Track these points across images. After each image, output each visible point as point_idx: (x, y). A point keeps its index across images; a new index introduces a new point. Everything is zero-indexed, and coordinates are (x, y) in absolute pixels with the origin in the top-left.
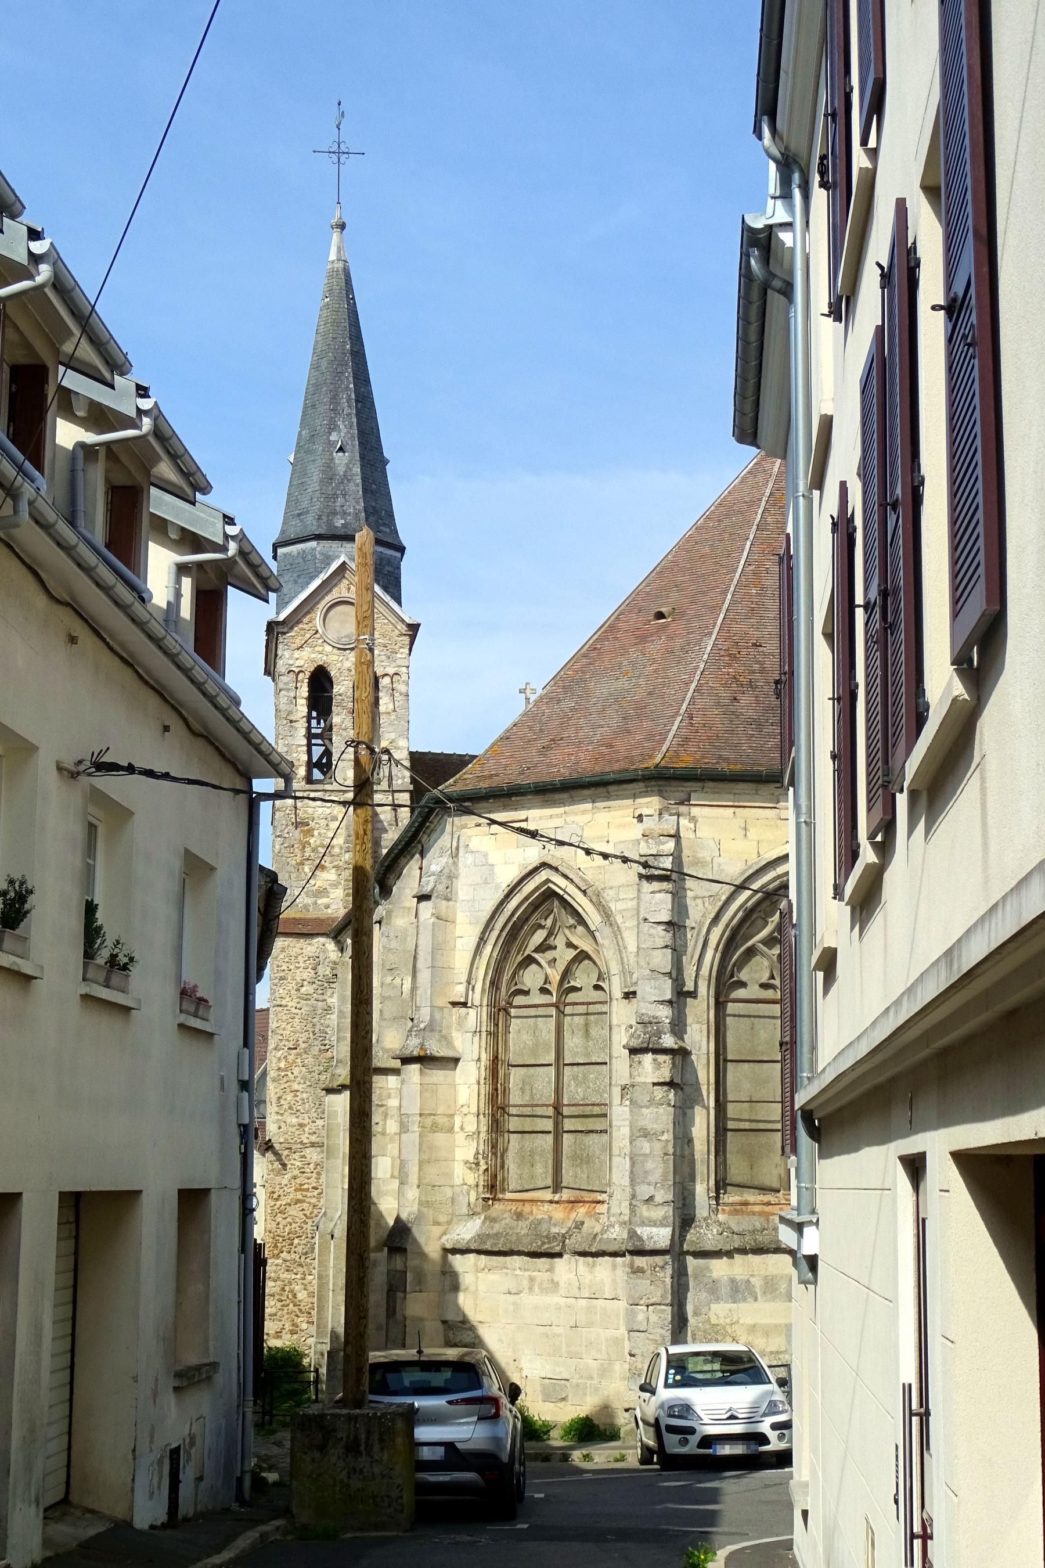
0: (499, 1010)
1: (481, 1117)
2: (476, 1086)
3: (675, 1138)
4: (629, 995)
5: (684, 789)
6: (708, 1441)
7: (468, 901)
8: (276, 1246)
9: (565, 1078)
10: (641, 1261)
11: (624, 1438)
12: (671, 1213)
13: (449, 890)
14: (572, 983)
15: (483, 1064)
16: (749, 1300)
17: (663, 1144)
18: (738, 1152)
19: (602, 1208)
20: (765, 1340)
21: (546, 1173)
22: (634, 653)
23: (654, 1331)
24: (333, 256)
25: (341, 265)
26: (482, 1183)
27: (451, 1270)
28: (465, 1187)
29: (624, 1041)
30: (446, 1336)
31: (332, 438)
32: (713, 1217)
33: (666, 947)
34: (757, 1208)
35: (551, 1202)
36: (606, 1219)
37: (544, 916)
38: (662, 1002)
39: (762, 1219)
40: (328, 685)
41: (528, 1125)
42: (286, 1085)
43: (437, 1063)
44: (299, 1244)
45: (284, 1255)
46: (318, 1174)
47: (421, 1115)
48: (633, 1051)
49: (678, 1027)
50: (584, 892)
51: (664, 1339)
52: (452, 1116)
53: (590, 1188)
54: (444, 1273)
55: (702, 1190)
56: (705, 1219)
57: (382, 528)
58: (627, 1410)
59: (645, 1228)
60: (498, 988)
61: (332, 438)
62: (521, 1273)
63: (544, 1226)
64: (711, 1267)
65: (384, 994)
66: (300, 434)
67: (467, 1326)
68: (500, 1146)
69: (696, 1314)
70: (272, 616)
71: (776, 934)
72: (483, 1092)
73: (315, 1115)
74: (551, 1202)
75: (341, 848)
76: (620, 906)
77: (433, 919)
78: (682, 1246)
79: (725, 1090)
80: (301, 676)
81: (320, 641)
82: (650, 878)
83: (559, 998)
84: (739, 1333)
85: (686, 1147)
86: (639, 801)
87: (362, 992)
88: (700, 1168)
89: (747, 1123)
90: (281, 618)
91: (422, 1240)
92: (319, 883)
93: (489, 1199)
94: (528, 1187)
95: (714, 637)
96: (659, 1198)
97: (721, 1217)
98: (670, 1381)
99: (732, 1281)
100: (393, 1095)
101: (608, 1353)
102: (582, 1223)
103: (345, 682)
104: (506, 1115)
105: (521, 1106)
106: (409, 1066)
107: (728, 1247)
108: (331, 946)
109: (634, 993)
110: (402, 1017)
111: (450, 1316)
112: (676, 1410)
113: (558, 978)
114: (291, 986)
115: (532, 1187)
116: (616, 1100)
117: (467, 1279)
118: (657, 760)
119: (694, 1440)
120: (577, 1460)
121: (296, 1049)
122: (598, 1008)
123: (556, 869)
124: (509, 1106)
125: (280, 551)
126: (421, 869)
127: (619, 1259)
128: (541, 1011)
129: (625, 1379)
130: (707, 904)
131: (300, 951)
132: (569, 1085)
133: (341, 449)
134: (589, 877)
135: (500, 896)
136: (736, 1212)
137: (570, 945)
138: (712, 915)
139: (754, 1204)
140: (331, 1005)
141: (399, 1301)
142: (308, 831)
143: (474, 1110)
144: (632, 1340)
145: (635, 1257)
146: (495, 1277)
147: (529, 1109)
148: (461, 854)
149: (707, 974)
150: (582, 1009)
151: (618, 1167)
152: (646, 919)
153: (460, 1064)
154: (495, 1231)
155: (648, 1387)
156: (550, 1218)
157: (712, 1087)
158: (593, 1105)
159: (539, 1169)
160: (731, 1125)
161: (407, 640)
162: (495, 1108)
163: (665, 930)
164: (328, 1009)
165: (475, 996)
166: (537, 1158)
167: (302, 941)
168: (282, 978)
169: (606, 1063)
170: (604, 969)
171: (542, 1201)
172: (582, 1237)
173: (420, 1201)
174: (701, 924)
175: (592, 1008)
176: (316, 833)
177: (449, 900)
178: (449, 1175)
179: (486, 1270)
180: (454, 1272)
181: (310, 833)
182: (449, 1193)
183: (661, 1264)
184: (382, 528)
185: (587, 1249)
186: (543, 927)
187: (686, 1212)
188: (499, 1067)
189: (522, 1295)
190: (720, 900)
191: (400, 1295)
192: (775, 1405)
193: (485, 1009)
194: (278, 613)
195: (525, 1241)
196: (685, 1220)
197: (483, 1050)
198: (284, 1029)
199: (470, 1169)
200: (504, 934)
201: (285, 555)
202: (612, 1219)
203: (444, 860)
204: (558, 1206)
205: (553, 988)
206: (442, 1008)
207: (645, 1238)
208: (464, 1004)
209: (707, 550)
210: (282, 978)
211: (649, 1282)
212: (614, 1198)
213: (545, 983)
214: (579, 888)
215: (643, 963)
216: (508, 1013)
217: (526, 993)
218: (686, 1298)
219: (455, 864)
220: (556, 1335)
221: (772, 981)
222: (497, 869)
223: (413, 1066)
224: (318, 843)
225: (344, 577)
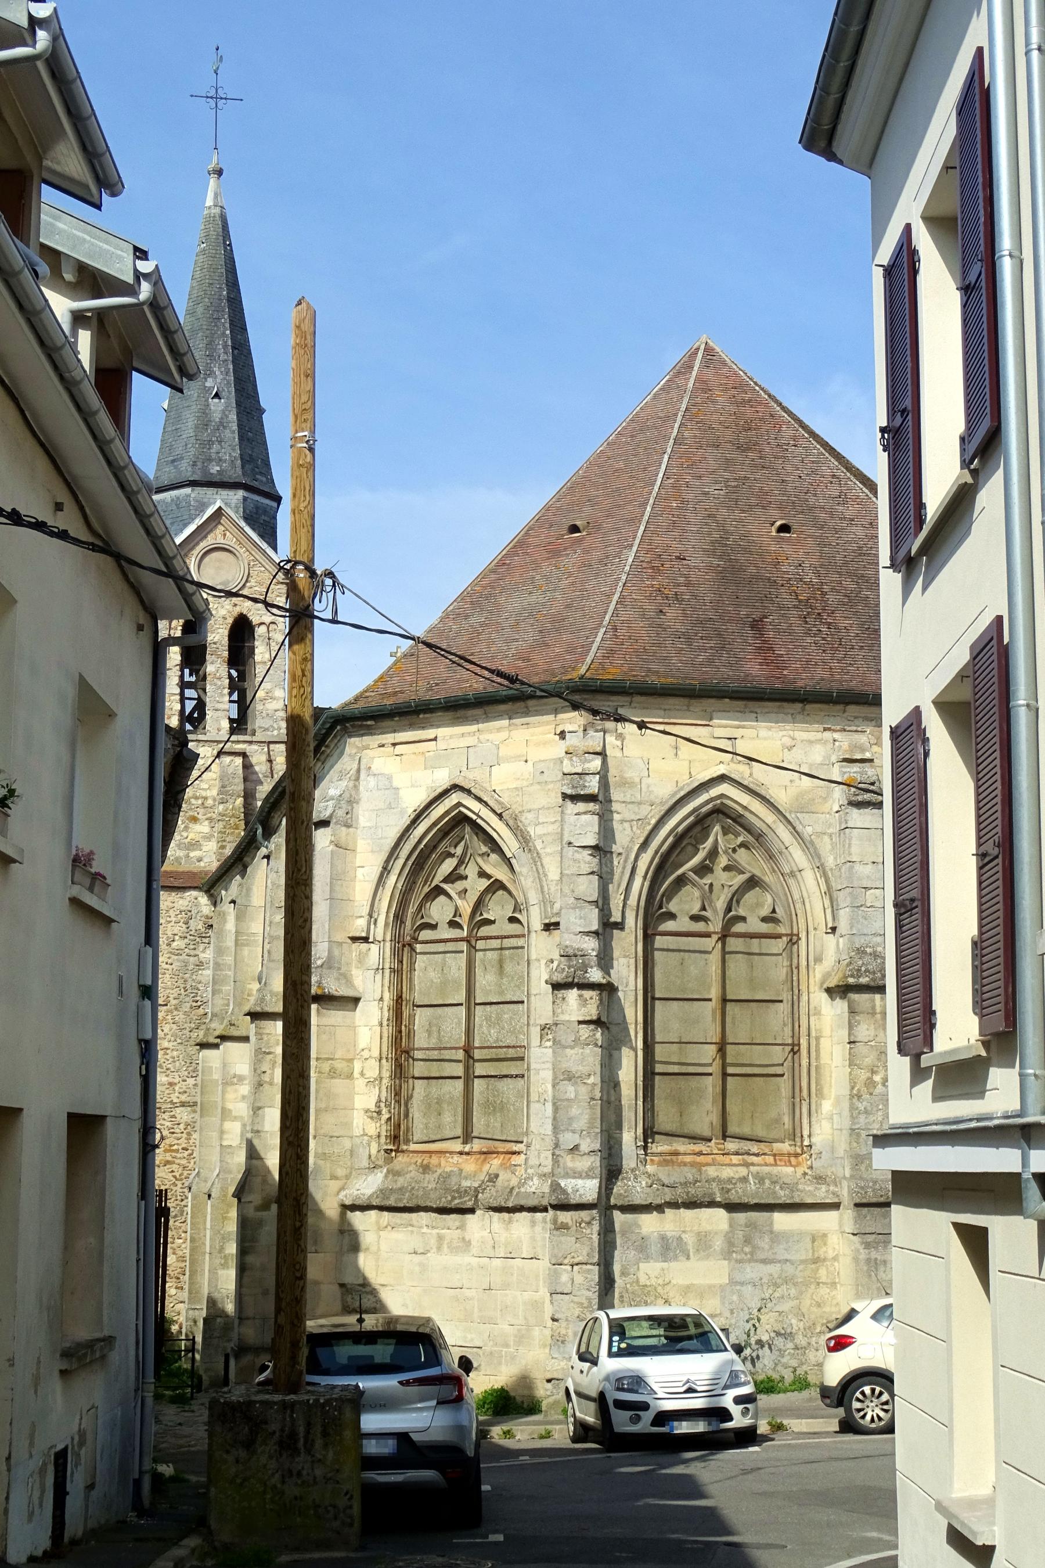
0: (404, 946)
1: (384, 1061)
3: (602, 1081)
4: (550, 927)
5: (610, 703)
6: (664, 1417)
7: (370, 828)
9: (477, 1019)
10: (565, 1217)
11: (546, 1412)
12: (598, 1164)
13: (349, 816)
14: (485, 916)
15: (386, 1003)
16: (682, 1258)
17: (590, 1088)
18: (666, 1098)
19: (519, 1160)
20: (698, 1302)
21: (455, 1121)
22: (546, 568)
23: (579, 1293)
24: (209, 202)
25: (217, 210)
26: (384, 1133)
28: (366, 1138)
29: (545, 976)
30: (343, 1301)
31: (208, 384)
32: (642, 1168)
33: (592, 873)
34: (688, 1159)
35: (461, 1153)
36: (523, 1171)
37: (453, 844)
38: (588, 933)
39: (694, 1170)
41: (435, 1070)
43: (335, 1003)
46: (189, 1134)
48: (557, 986)
49: (605, 960)
50: (500, 816)
51: (590, 1303)
52: (351, 1061)
53: (504, 1138)
54: (342, 1232)
55: (629, 1138)
56: (633, 1170)
57: (258, 477)
58: (549, 1381)
59: (569, 1180)
60: (402, 922)
61: (208, 384)
62: (429, 1231)
63: (454, 1180)
64: (640, 1223)
65: (272, 933)
67: (368, 1289)
68: (404, 1093)
69: (623, 1274)
71: (707, 862)
72: (385, 1035)
73: (186, 1073)
74: (461, 1153)
75: (214, 800)
76: (540, 830)
77: (332, 847)
78: (608, 1199)
79: (653, 1030)
82: (575, 798)
83: (470, 931)
84: (671, 1295)
85: (612, 1092)
86: (561, 716)
87: (299, 870)
88: (628, 1115)
89: (676, 1067)
92: (191, 836)
93: (391, 1150)
95: (635, 549)
96: (584, 1147)
97: (650, 1168)
98: (615, 1349)
99: (663, 1238)
101: (525, 1318)
102: (497, 1176)
103: (220, 631)
104: (411, 1060)
105: (427, 1049)
107: (659, 1201)
108: (203, 899)
109: (557, 925)
111: (349, 1279)
112: (625, 1382)
113: (469, 910)
115: (439, 1137)
116: (535, 1040)
117: (367, 1238)
118: (583, 671)
119: (648, 1416)
120: (496, 1437)
122: (513, 942)
123: (468, 792)
124: (414, 1049)
127: (539, 1215)
128: (450, 947)
129: (545, 1346)
130: (635, 828)
131: (172, 905)
132: (481, 1026)
133: (217, 396)
134: (505, 799)
136: (665, 1163)
137: (483, 874)
138: (642, 840)
139: (685, 1154)
140: (203, 960)
143: (376, 1054)
144: (555, 1303)
145: (558, 1212)
146: (398, 1236)
147: (436, 1052)
149: (635, 904)
150: (496, 943)
151: (537, 1114)
152: (570, 843)
153: (360, 1004)
154: (399, 1185)
155: (588, 1356)
156: (461, 1170)
157: (640, 1027)
158: (509, 1047)
159: (447, 1118)
160: (659, 1068)
163: (591, 855)
164: (200, 965)
166: (445, 1106)
169: (522, 1002)
170: (521, 899)
171: (451, 1153)
172: (497, 1191)
174: (628, 850)
175: (507, 943)
177: (348, 826)
178: (348, 1125)
179: (389, 1228)
182: (347, 1144)
183: (587, 1219)
184: (258, 477)
185: (503, 1204)
186: (452, 856)
187: (611, 1163)
188: (404, 1008)
189: (429, 1255)
190: (649, 824)
192: (737, 1377)
193: (388, 944)
195: (432, 1196)
196: (612, 1172)
197: (386, 989)
199: (372, 1118)
200: (410, 863)
202: (530, 1171)
203: (344, 784)
204: (469, 1157)
205: (464, 921)
206: (340, 944)
207: (570, 1191)
208: (366, 939)
209: (621, 465)
211: (574, 1239)
212: (532, 1148)
213: (455, 916)
214: (494, 811)
215: (566, 890)
216: (413, 950)
217: (433, 927)
218: (613, 1257)
219: (356, 787)
220: (467, 1299)
221: (703, 913)
222: (402, 793)
225: (220, 523)
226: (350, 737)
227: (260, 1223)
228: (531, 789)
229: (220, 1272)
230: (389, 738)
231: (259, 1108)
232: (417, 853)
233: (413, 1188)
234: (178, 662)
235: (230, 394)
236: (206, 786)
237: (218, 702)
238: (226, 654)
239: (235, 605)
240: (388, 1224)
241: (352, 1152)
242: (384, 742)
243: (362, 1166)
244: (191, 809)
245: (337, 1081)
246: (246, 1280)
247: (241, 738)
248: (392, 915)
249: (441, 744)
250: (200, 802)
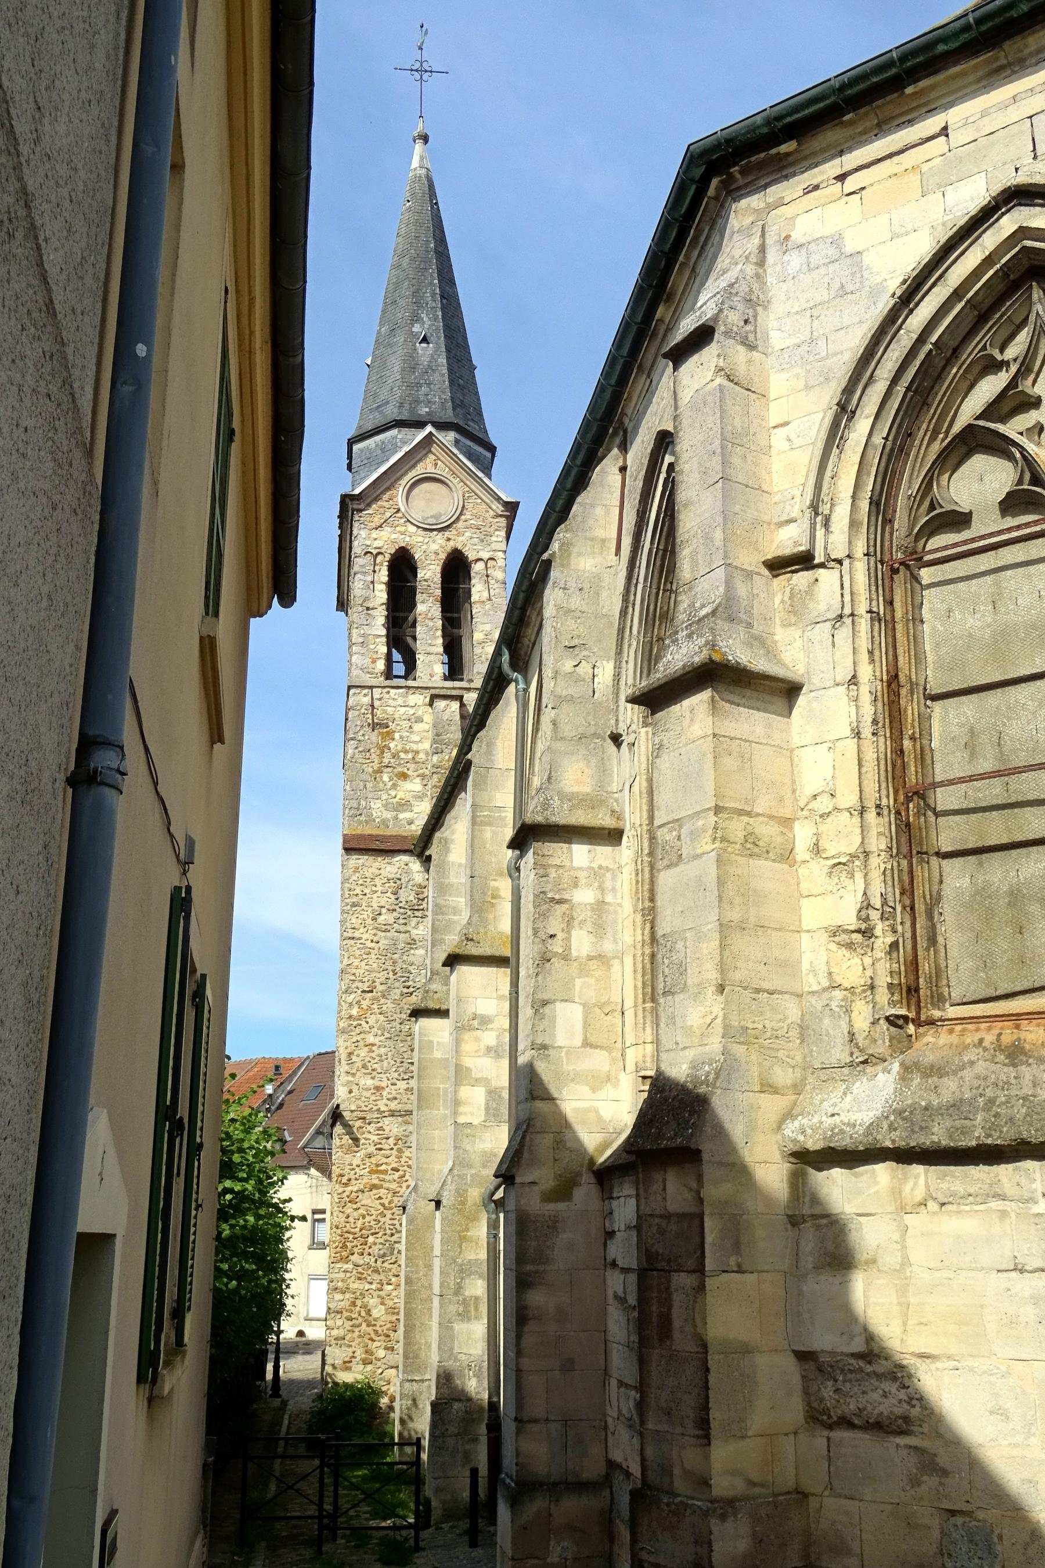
2: (852, 743)
8: (344, 1247)
13: (749, 328)
24: (415, 163)
25: (423, 171)
26: (883, 979)
27: (817, 1211)
28: (838, 994)
31: (414, 329)
37: (999, 340)
40: (410, 577)
42: (359, 1038)
43: (748, 692)
44: (375, 1244)
45: (355, 1258)
46: (400, 1151)
47: (718, 810)
52: (787, 822)
54: (794, 1221)
60: (888, 521)
61: (414, 329)
65: (559, 691)
66: (379, 332)
67: (881, 1366)
70: (347, 490)
72: (870, 755)
73: (396, 1075)
75: (427, 754)
77: (718, 381)
80: (380, 558)
81: (402, 521)
90: (357, 491)
91: (737, 1129)
92: (401, 795)
93: (906, 1018)
94: (1004, 988)
100: (583, 881)
104: (930, 813)
106: (676, 709)
108: (416, 865)
110: (595, 735)
114: (367, 914)
115: (1027, 985)
121: (372, 991)
125: (356, 447)
126: (623, 469)
131: (377, 872)
135: (884, 304)
140: (416, 938)
141: (678, 1299)
142: (388, 733)
143: (849, 798)
148: (771, 257)
153: (802, 701)
161: (503, 522)
162: (901, 798)
164: (412, 943)
165: (832, 538)
167: (380, 859)
168: (354, 905)
173: (726, 1027)
176: (397, 736)
177: (752, 347)
178: (790, 966)
179: (932, 1206)
180: (827, 1216)
181: (390, 735)
182: (792, 1010)
184: (470, 423)
186: (993, 366)
188: (903, 702)
191: (682, 1280)
193: (861, 567)
194: (354, 487)
197: (864, 656)
198: (357, 968)
199: (850, 946)
201: (361, 450)
206: (749, 575)
208: (804, 561)
210: (354, 905)
213: (1020, 482)
216: (916, 579)
222: (867, 259)
223: (687, 703)
224: (399, 748)
225: (430, 451)
226: (736, 200)
227: (553, 1224)
229: (458, 1327)
230: (832, 168)
231: (545, 1003)
233: (992, 1101)
234: (385, 601)
235: (439, 338)
236: (417, 739)
237: (430, 645)
238: (439, 592)
239: (449, 539)
240: (930, 1196)
241: (803, 1030)
242: (815, 182)
243: (834, 1061)
244: (400, 764)
245: (763, 865)
246: (528, 1341)
247: (457, 684)
248: (864, 505)
249: (957, 137)
250: (410, 756)
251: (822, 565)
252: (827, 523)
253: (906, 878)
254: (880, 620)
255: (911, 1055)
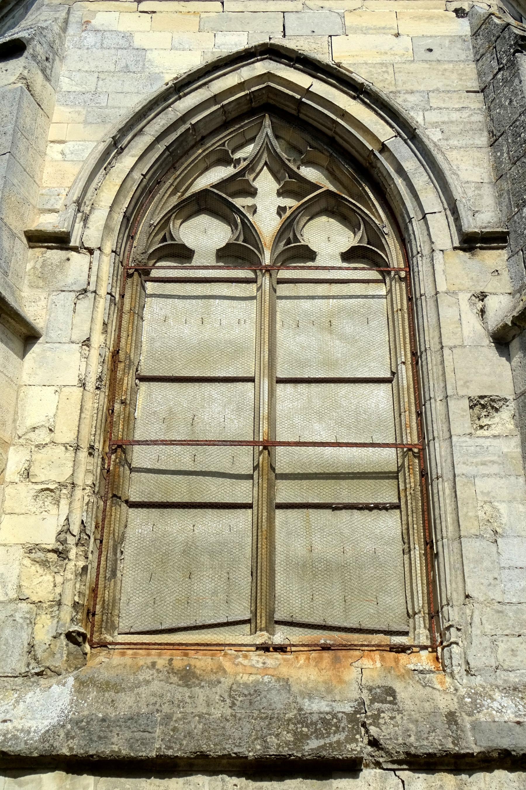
2: (77, 392)
26: (68, 601)
28: (24, 606)
35: (265, 648)
72: (89, 405)
76: (432, 117)
93: (84, 635)
148: (71, 31)
153: (37, 348)
165: (87, 232)
197: (98, 327)
199: (44, 564)
206: (13, 236)
222: (150, 55)
228: (413, 67)
232: (182, 129)
233: (168, 717)
243: (8, 671)
248: (118, 217)
251: (75, 249)
252: (86, 219)
253: (100, 515)
254: (115, 305)
255: (85, 672)
